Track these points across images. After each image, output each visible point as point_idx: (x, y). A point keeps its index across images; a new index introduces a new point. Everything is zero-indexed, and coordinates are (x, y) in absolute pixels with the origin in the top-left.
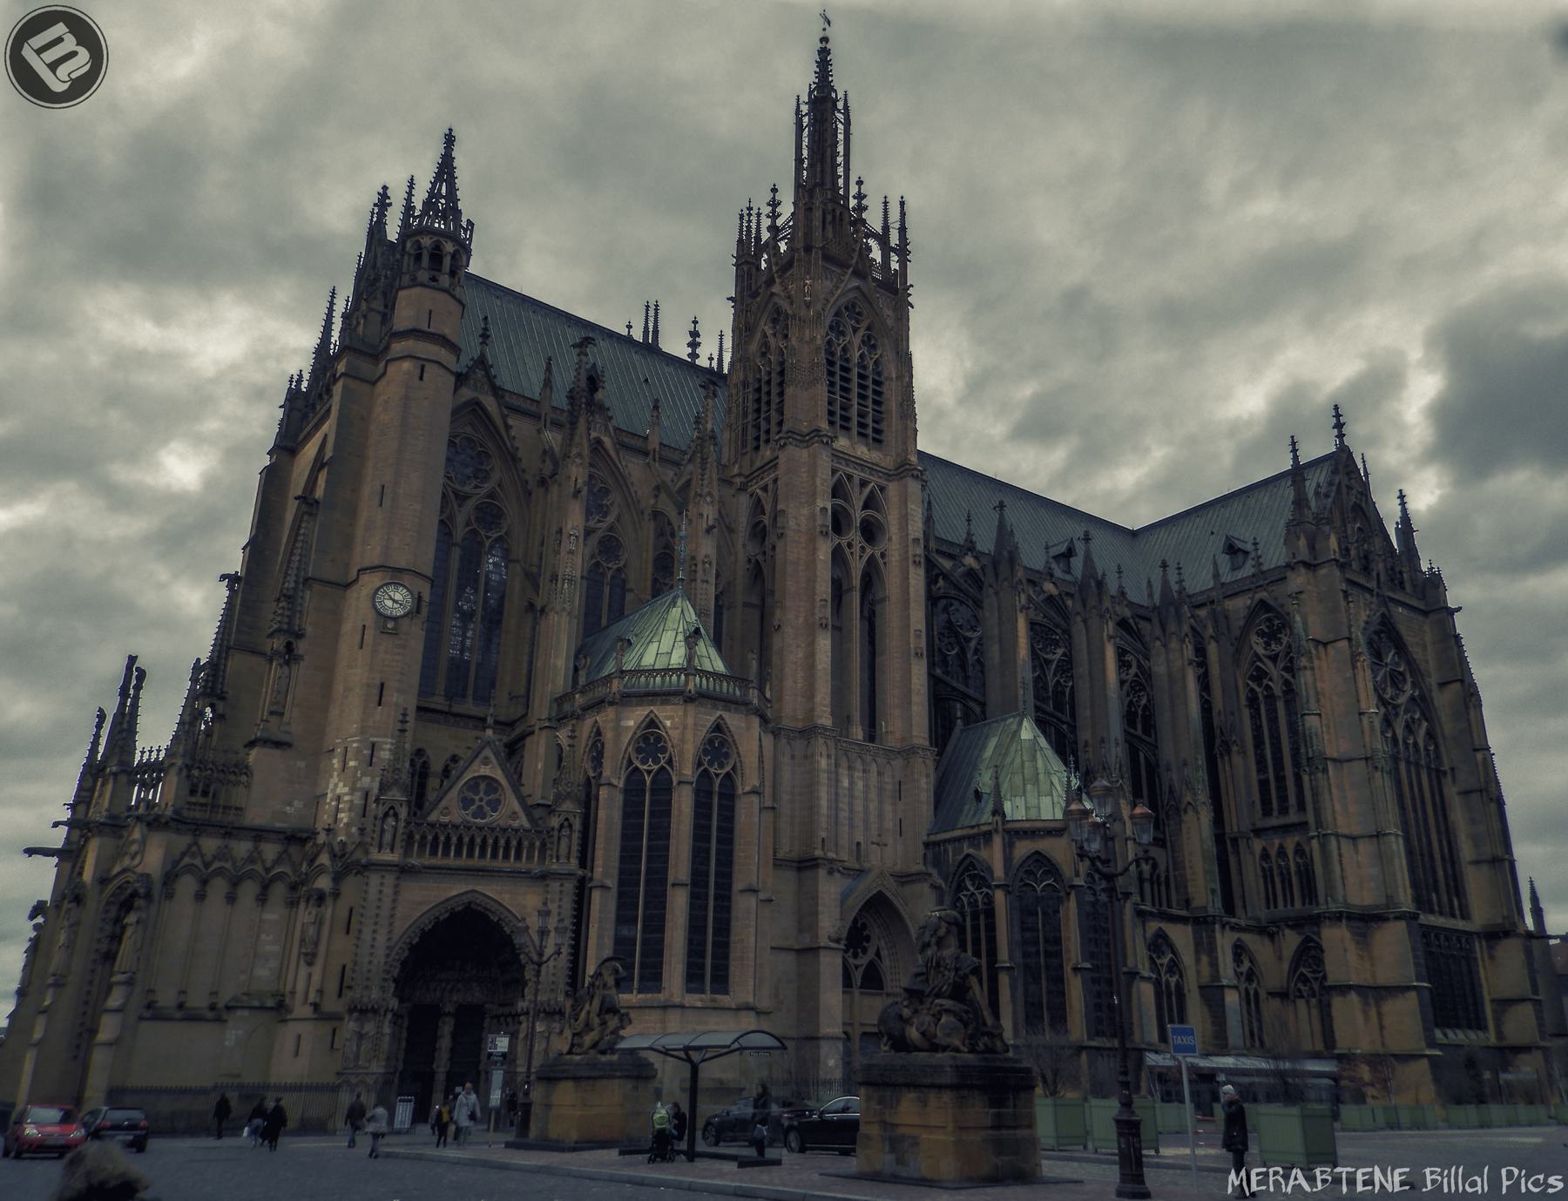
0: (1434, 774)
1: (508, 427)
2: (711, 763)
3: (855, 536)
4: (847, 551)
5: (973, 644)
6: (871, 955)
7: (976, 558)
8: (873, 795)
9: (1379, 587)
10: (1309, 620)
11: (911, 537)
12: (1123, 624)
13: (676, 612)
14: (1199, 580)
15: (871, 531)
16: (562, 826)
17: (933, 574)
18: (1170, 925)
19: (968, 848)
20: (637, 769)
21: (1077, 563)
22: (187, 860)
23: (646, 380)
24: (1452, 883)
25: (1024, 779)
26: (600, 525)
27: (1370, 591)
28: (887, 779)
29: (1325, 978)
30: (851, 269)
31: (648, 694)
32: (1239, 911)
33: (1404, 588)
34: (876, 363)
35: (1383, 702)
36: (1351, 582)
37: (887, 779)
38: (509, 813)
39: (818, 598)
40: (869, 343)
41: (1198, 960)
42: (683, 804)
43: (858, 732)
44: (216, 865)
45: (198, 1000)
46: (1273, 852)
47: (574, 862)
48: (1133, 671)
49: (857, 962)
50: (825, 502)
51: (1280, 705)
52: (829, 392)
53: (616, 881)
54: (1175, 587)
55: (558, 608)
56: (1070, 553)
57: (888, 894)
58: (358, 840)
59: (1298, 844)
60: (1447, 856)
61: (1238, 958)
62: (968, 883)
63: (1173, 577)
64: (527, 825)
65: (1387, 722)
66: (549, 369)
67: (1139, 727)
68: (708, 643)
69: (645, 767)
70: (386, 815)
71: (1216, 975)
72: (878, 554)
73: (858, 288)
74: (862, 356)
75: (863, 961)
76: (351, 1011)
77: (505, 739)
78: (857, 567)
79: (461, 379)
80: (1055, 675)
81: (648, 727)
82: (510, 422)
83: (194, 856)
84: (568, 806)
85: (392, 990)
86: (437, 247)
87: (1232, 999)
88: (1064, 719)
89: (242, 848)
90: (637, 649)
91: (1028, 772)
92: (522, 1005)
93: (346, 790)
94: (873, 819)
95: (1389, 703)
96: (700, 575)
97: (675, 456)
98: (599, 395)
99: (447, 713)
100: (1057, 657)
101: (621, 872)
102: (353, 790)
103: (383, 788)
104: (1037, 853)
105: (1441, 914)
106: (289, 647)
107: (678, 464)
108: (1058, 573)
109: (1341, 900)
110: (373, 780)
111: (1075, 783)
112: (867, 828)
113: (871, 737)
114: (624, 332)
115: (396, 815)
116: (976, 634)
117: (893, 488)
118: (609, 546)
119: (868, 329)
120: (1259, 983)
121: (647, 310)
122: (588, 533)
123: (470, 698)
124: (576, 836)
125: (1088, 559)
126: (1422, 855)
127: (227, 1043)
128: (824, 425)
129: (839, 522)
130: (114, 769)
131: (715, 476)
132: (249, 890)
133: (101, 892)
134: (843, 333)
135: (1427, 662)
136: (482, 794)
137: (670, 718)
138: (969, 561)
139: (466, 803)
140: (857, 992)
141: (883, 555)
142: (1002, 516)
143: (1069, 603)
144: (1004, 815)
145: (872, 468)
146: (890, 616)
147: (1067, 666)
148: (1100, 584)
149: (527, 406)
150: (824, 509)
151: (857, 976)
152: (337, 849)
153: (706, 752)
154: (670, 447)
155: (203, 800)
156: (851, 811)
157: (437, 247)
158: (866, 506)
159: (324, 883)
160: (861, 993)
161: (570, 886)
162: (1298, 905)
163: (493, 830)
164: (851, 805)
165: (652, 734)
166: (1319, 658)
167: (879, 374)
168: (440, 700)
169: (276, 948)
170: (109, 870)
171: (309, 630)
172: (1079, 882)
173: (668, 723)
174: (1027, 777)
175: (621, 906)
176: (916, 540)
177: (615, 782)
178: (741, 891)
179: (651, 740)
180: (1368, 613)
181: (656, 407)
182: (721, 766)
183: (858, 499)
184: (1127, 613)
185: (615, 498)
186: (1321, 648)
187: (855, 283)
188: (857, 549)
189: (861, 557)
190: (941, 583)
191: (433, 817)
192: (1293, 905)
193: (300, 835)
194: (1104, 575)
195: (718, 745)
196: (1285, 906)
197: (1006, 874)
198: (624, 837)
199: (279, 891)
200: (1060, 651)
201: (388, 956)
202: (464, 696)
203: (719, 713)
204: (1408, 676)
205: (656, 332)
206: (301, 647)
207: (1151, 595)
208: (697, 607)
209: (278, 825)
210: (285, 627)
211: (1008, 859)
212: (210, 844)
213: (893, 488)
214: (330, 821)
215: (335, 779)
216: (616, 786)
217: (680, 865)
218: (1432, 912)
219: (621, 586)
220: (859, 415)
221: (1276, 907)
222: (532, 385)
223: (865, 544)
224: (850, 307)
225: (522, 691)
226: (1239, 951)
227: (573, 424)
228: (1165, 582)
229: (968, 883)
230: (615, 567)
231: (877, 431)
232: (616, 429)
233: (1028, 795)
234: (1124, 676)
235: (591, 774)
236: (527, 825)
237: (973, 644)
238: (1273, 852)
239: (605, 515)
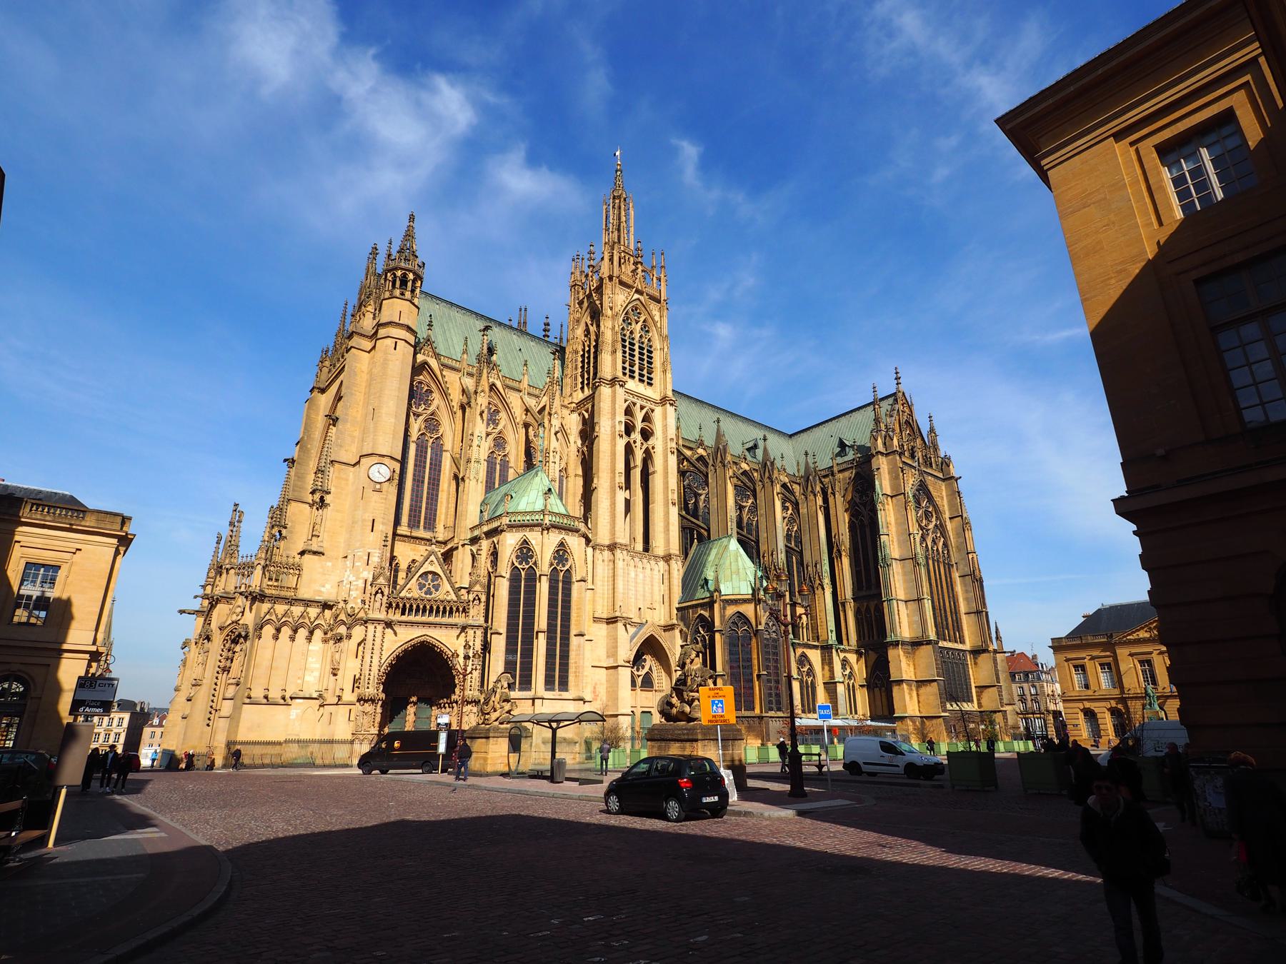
0: (947, 566)
1: (443, 376)
2: (558, 564)
3: (636, 436)
4: (633, 445)
5: (703, 497)
6: (646, 669)
7: (704, 449)
8: (648, 580)
9: (919, 466)
10: (883, 484)
11: (669, 437)
12: (784, 486)
13: (537, 479)
14: (824, 462)
15: (646, 435)
16: (474, 599)
17: (681, 458)
18: (809, 650)
19: (700, 610)
20: (516, 567)
21: (759, 452)
22: (268, 617)
23: (520, 350)
24: (956, 625)
26: (494, 430)
27: (914, 468)
28: (656, 572)
29: (889, 677)
30: (634, 289)
31: (522, 526)
32: (845, 642)
33: (932, 467)
34: (649, 340)
35: (922, 528)
36: (904, 462)
37: (656, 572)
38: (445, 592)
39: (617, 472)
40: (645, 328)
41: (823, 669)
42: (543, 588)
43: (639, 546)
44: (284, 619)
45: (275, 694)
46: (863, 610)
47: (482, 619)
48: (790, 512)
49: (639, 673)
50: (621, 417)
51: (868, 530)
52: (623, 356)
53: (505, 630)
54: (812, 466)
55: (471, 478)
56: (755, 446)
57: (657, 636)
58: (361, 607)
59: (876, 604)
60: (953, 611)
61: (844, 667)
62: (700, 629)
63: (810, 460)
64: (455, 599)
65: (923, 538)
66: (466, 344)
67: (793, 543)
68: (556, 497)
69: (521, 566)
70: (377, 593)
71: (832, 676)
72: (650, 448)
73: (638, 299)
74: (641, 337)
75: (643, 672)
76: (359, 700)
77: (442, 551)
78: (639, 455)
79: (417, 348)
80: (747, 514)
81: (521, 544)
82: (444, 373)
83: (271, 615)
84: (478, 588)
85: (382, 689)
86: (404, 276)
87: (841, 689)
88: (752, 538)
89: (297, 610)
90: (515, 500)
91: (734, 567)
92: (453, 697)
93: (354, 579)
94: (648, 595)
95: (924, 528)
96: (551, 459)
97: (537, 392)
98: (494, 358)
99: (406, 536)
100: (749, 504)
101: (508, 625)
102: (358, 578)
103: (375, 578)
104: (738, 612)
105: (950, 641)
106: (322, 499)
107: (538, 397)
108: (749, 458)
109: (899, 635)
110: (369, 573)
111: (759, 574)
112: (644, 600)
113: (646, 549)
114: (508, 323)
115: (382, 593)
116: (704, 492)
117: (658, 410)
118: (500, 442)
119: (644, 322)
120: (855, 680)
121: (520, 311)
122: (488, 435)
123: (422, 527)
124: (482, 604)
125: (765, 450)
126: (940, 610)
127: (291, 717)
128: (620, 374)
129: (629, 429)
130: (228, 566)
131: (559, 403)
132: (303, 633)
133: (221, 634)
134: (630, 324)
135: (944, 506)
136: (429, 582)
137: (534, 537)
138: (701, 451)
139: (421, 587)
140: (638, 690)
141: (653, 448)
142: (718, 426)
143: (755, 474)
144: (720, 592)
145: (648, 399)
146: (657, 482)
147: (754, 509)
148: (772, 463)
149: (454, 364)
150: (620, 422)
151: (639, 681)
152: (349, 611)
153: (555, 558)
154: (533, 387)
155: (276, 584)
156: (636, 591)
157: (404, 276)
158: (643, 421)
159: (342, 630)
160: (641, 690)
161: (479, 633)
162: (875, 637)
163: (436, 601)
164: (636, 587)
165: (525, 548)
166: (888, 504)
167: (651, 347)
168: (406, 528)
169: (318, 666)
170: (224, 623)
171: (333, 490)
172: (760, 628)
173: (533, 542)
175: (508, 643)
176: (672, 439)
177: (504, 575)
178: (575, 635)
179: (525, 551)
180: (913, 479)
181: (526, 365)
182: (564, 566)
183: (639, 415)
184: (786, 480)
185: (503, 415)
186: (889, 498)
187: (636, 296)
188: (638, 444)
189: (641, 449)
190: (685, 463)
191: (402, 594)
192: (873, 637)
193: (329, 603)
194: (774, 459)
195: (561, 553)
196: (869, 639)
197: (722, 624)
198: (510, 605)
199: (318, 634)
200: (750, 501)
201: (379, 671)
202: (418, 527)
203: (562, 536)
204: (934, 514)
205: (525, 323)
206: (328, 499)
207: (798, 470)
208: (550, 477)
209: (317, 598)
210: (320, 488)
211: (722, 616)
212: (280, 608)
213: (658, 410)
214: (347, 596)
215: (348, 573)
216: (504, 577)
217: (541, 621)
218: (945, 640)
219: (505, 465)
220: (639, 370)
221: (864, 639)
222: (457, 352)
223: (643, 441)
224: (635, 309)
225: (452, 525)
226: (845, 663)
227: (480, 374)
228: (807, 463)
229: (700, 629)
230: (503, 454)
231: (650, 379)
232: (503, 376)
233: (733, 580)
234: (784, 515)
235: (491, 570)
236: (455, 599)
237: (703, 497)
238: (863, 610)
239: (497, 424)
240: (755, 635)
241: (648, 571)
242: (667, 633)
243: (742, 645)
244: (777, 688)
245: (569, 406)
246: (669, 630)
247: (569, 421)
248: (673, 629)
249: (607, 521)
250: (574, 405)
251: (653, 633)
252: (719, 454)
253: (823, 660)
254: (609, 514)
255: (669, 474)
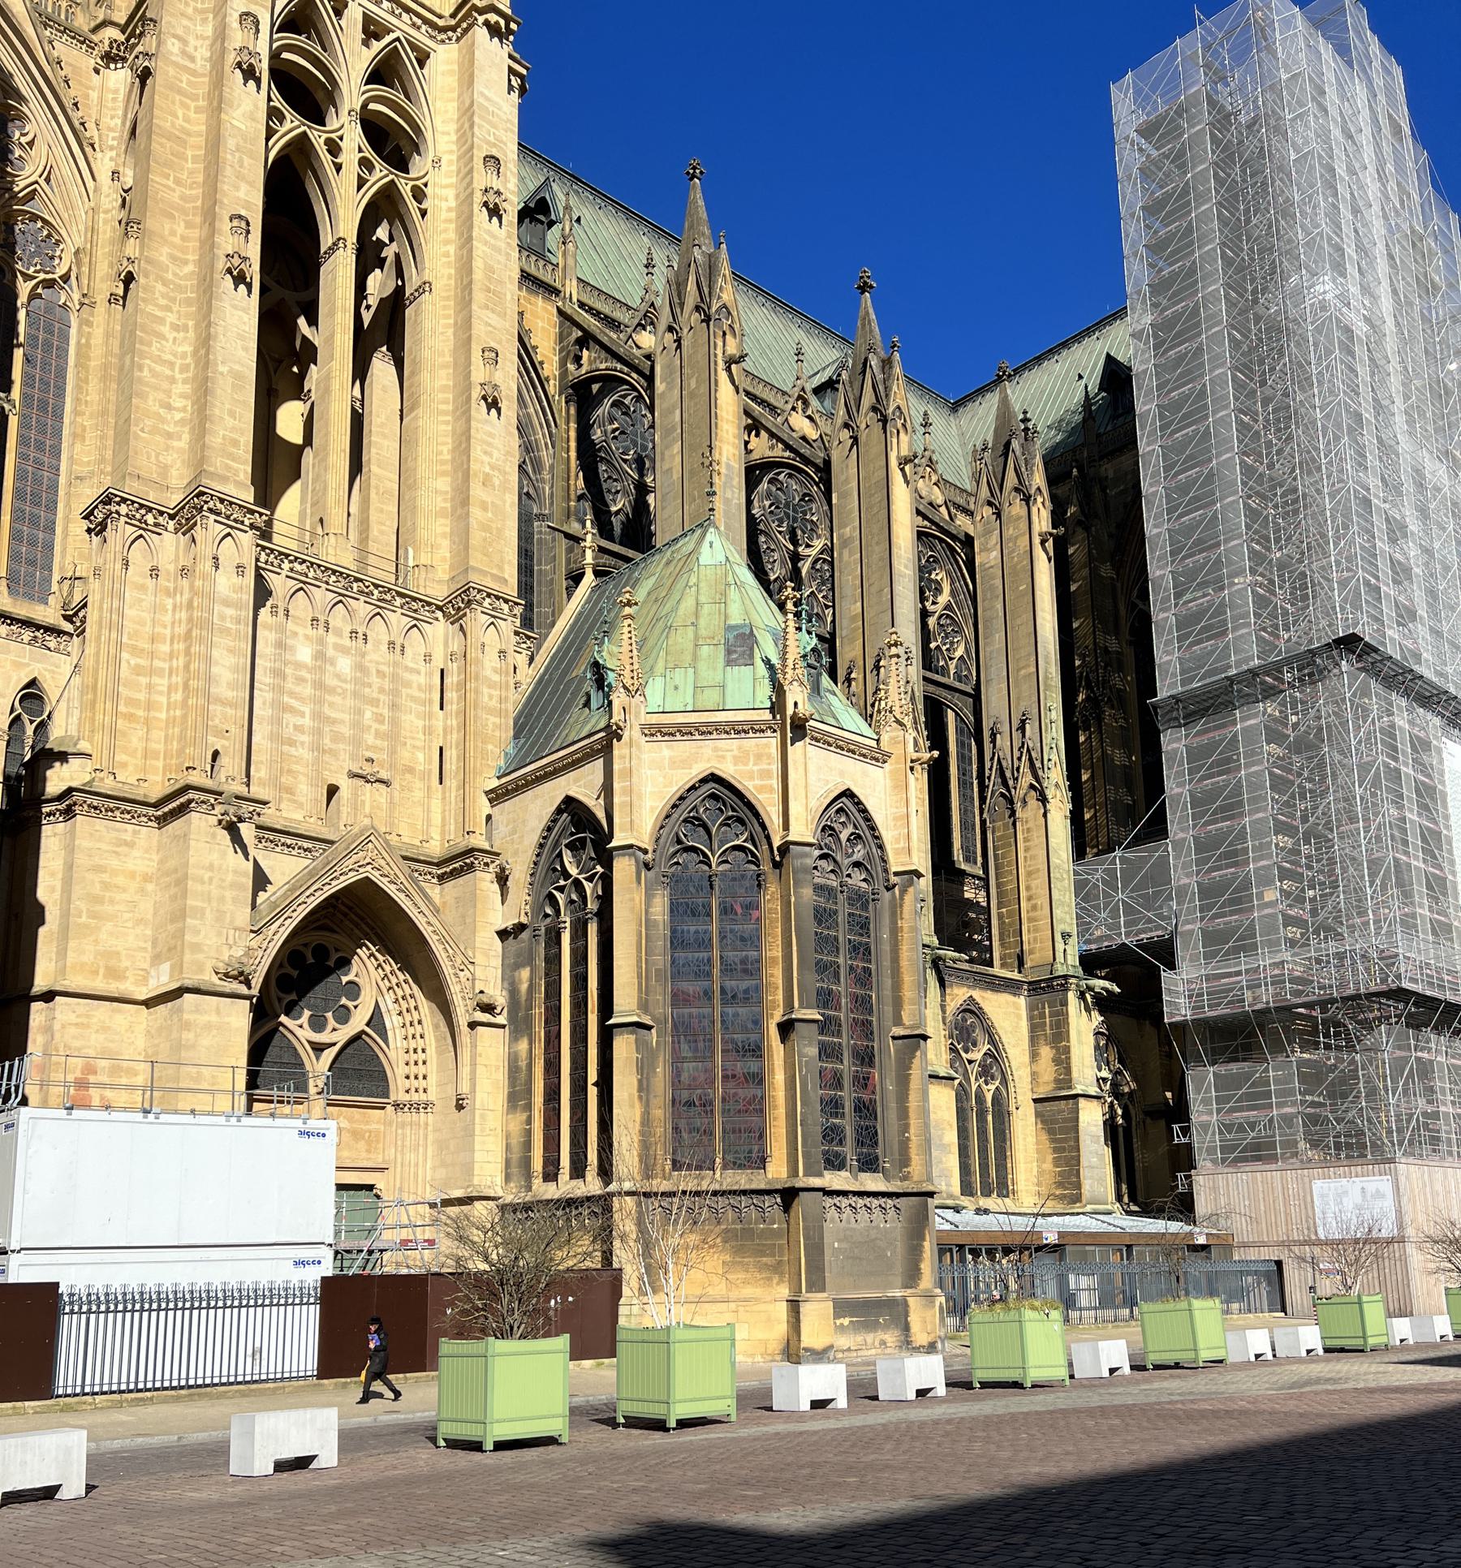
18: (989, 994)
25: (696, 638)
62: (567, 857)
104: (713, 778)
156: (318, 716)
174: (703, 632)
229: (567, 857)
233: (702, 666)
240: (777, 865)
241: (377, 654)
242: (450, 885)
243: (725, 910)
244: (863, 1082)
245: (95, 38)
246: (455, 874)
247: (94, 95)
248: (470, 868)
249: (178, 416)
250: (112, 33)
251: (375, 876)
252: (692, 279)
253: (1035, 1029)
254: (187, 388)
255: (475, 287)
